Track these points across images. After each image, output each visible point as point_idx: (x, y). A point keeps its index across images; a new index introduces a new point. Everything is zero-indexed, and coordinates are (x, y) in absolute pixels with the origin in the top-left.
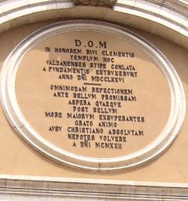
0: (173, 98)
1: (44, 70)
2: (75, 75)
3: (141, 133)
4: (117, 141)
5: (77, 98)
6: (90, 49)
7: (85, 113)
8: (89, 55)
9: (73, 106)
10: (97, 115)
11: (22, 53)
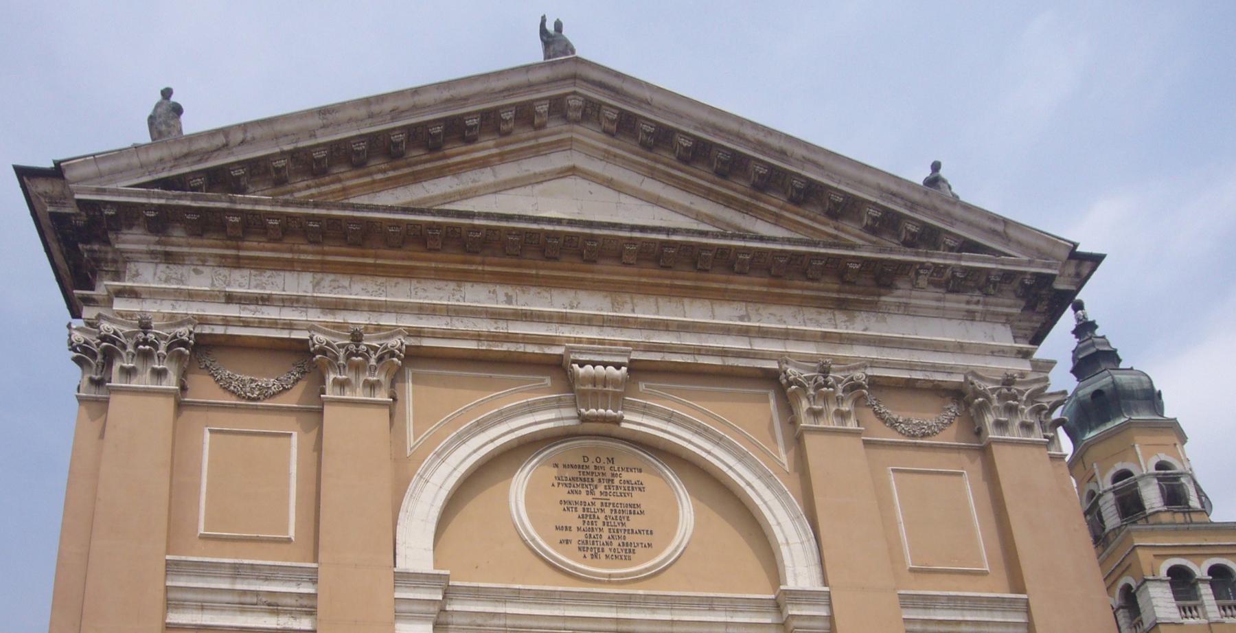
0: (681, 512)
1: (553, 485)
2: (584, 491)
3: (650, 545)
4: (627, 553)
5: (586, 513)
6: (598, 465)
7: (594, 527)
8: (597, 471)
9: (582, 520)
10: (606, 528)
11: (531, 470)
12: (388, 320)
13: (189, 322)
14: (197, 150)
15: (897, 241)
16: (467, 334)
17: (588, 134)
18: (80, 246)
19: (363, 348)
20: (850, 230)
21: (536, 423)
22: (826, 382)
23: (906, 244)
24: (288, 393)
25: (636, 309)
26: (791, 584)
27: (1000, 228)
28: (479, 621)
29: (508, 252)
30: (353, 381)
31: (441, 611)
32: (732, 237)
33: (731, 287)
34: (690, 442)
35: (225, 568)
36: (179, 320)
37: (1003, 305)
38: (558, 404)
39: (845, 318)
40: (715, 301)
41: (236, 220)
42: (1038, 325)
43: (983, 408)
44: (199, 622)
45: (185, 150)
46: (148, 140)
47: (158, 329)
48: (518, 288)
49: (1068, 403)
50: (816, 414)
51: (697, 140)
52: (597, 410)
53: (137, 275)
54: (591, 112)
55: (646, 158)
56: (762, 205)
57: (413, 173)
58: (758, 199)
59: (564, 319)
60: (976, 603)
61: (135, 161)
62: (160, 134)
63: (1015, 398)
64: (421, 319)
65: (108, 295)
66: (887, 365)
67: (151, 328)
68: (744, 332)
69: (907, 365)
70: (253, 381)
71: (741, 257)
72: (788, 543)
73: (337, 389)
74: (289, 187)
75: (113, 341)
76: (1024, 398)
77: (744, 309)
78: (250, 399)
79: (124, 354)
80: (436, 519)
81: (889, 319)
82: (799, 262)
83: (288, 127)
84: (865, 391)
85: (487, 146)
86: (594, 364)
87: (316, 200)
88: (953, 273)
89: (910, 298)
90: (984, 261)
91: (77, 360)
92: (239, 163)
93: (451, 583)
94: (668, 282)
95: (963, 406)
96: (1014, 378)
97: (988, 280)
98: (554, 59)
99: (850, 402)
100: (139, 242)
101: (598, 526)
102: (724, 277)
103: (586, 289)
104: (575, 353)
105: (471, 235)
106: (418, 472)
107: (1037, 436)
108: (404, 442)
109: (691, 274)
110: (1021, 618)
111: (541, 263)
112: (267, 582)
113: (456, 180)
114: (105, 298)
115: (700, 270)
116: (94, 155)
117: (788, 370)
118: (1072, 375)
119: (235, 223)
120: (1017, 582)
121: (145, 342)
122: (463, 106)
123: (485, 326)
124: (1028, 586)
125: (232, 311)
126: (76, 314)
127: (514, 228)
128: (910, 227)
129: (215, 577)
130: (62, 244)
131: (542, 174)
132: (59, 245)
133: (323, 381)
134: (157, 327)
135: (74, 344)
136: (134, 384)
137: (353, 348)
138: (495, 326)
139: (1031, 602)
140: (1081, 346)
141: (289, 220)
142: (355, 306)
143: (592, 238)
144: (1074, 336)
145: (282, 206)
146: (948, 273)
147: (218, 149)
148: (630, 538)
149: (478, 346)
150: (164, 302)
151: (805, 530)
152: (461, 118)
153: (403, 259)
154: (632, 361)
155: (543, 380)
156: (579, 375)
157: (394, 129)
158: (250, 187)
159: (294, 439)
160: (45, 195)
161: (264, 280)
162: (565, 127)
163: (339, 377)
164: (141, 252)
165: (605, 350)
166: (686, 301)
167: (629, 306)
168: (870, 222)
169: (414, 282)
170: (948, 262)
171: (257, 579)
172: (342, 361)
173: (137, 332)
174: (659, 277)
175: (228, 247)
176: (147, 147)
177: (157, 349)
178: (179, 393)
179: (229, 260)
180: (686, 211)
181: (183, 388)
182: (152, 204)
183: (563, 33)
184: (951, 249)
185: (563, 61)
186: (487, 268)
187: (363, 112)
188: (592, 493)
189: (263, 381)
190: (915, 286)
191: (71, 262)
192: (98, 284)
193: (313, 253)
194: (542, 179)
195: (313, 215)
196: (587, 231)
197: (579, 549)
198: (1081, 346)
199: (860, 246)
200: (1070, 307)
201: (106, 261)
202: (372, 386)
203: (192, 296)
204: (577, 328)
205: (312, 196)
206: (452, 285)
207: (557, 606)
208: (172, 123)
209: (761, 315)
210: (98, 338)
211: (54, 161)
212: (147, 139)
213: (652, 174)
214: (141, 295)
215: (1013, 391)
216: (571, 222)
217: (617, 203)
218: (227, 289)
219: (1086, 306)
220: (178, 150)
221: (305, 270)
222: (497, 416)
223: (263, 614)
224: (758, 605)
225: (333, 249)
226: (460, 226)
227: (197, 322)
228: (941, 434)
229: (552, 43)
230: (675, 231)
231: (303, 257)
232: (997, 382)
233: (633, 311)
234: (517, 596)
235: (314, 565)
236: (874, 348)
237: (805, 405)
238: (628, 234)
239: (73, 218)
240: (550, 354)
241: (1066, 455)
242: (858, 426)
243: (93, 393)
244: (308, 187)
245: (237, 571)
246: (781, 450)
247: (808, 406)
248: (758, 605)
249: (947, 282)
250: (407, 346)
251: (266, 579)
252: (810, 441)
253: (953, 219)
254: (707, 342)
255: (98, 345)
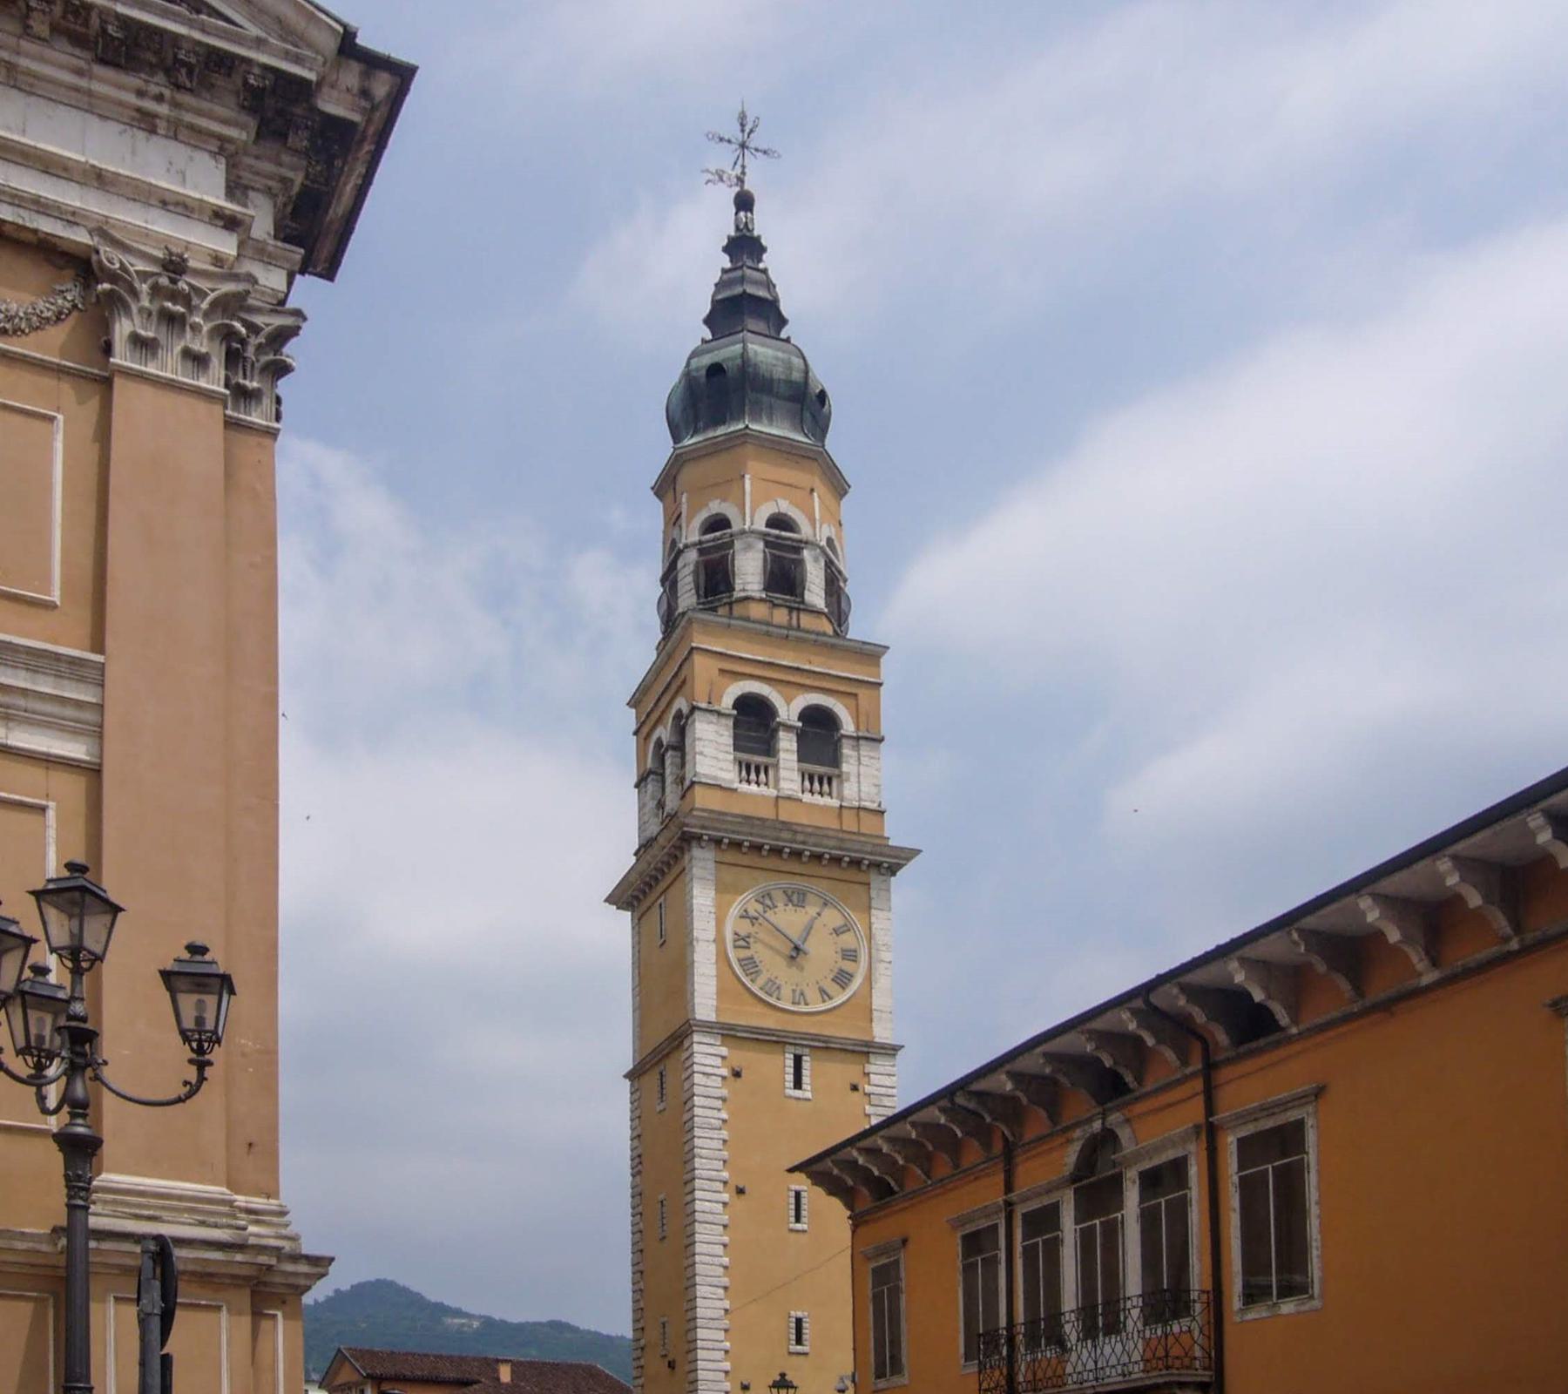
43: (114, 304)
63: (186, 300)
76: (205, 305)
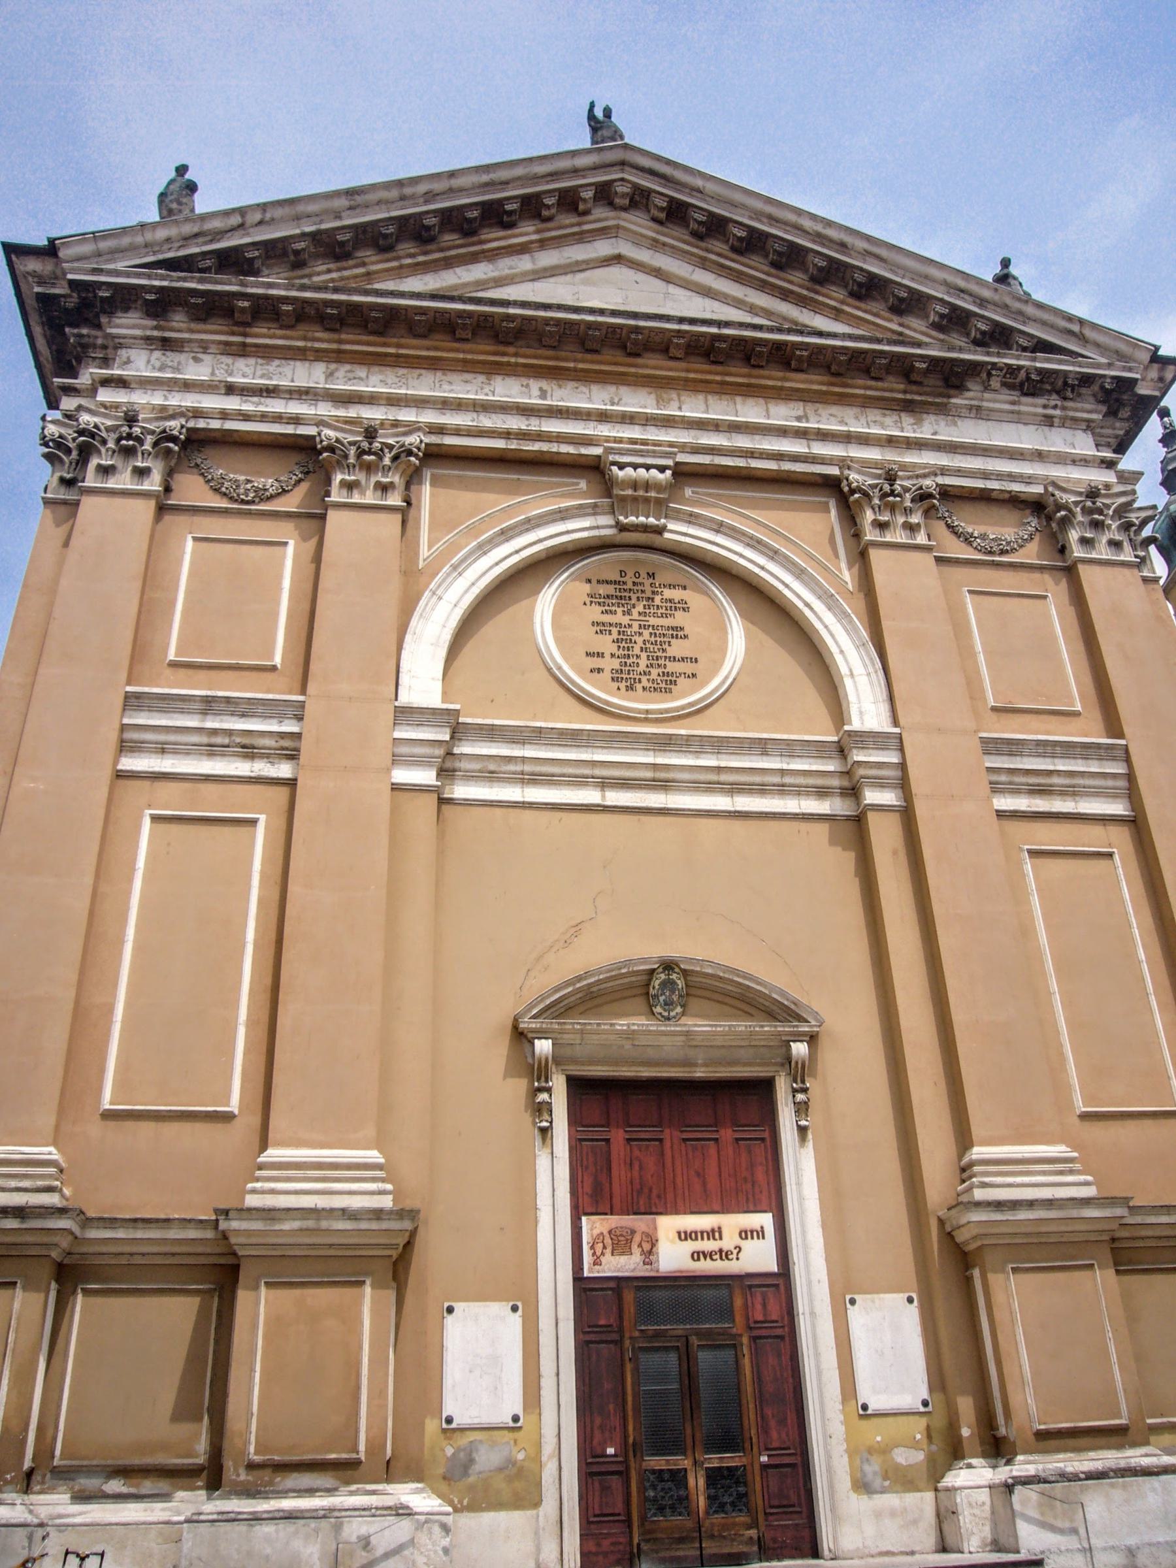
0: (730, 636)
1: (585, 604)
2: (619, 610)
3: (694, 675)
4: (667, 684)
5: (621, 636)
6: (636, 580)
7: (630, 653)
8: (635, 588)
9: (616, 644)
10: (644, 655)
11: (560, 586)
12: (407, 415)
13: (182, 415)
14: (210, 230)
15: (966, 340)
16: (494, 432)
17: (636, 222)
18: (67, 330)
19: (376, 445)
20: (916, 327)
21: (568, 532)
22: (892, 491)
23: (977, 343)
24: (288, 495)
25: (684, 407)
26: (856, 724)
27: (1076, 328)
28: (492, 767)
29: (544, 343)
30: (363, 482)
31: (448, 754)
32: (789, 331)
33: (788, 384)
34: (741, 556)
35: (195, 701)
36: (171, 412)
37: (1083, 411)
38: (595, 510)
39: (912, 421)
40: (769, 400)
41: (246, 304)
42: (1121, 433)
43: (1066, 522)
44: (157, 769)
45: (196, 229)
46: (158, 219)
47: (147, 423)
48: (555, 382)
49: (1159, 518)
50: (882, 526)
51: (751, 230)
52: (637, 518)
53: (128, 361)
54: (639, 199)
55: (697, 247)
56: (821, 298)
57: (445, 259)
58: (817, 292)
59: (603, 417)
60: (1068, 750)
61: (139, 239)
62: (171, 212)
63: (1101, 512)
64: (444, 414)
65: (92, 384)
66: (959, 472)
67: (137, 421)
68: (802, 434)
69: (980, 473)
70: (248, 481)
71: (798, 353)
72: (852, 675)
73: (344, 492)
74: (307, 271)
75: (93, 435)
76: (1111, 512)
77: (802, 409)
78: (243, 502)
79: (103, 450)
80: (448, 643)
81: (959, 423)
82: (861, 360)
83: (312, 208)
84: (935, 501)
85: (527, 231)
86: (635, 466)
87: (336, 284)
88: (1027, 374)
89: (982, 400)
90: (1060, 362)
91: (48, 456)
92: (253, 244)
93: (461, 720)
94: (718, 378)
95: (1044, 520)
96: (1099, 490)
97: (1065, 384)
98: (602, 145)
99: (919, 513)
100: (133, 327)
101: (634, 653)
102: (780, 374)
103: (629, 385)
104: (615, 453)
105: (505, 324)
106: (431, 586)
107: (1127, 555)
108: (417, 554)
109: (745, 370)
110: (1119, 768)
111: (580, 356)
112: (243, 719)
113: (491, 266)
114: (89, 387)
115: (754, 366)
116: (93, 233)
117: (851, 477)
118: (1162, 489)
119: (245, 307)
120: (1113, 726)
121: (129, 436)
122: (503, 190)
123: (515, 423)
124: (1126, 730)
125: (233, 403)
126: (53, 404)
127: (552, 318)
128: (979, 325)
129: (182, 712)
130: (46, 328)
131: (584, 262)
132: (43, 329)
133: (328, 481)
134: (146, 420)
135: (47, 439)
136: (111, 484)
137: (365, 445)
138: (527, 423)
139: (1131, 750)
140: (1170, 455)
141: (305, 305)
142: (371, 400)
143: (637, 330)
144: (1161, 445)
145: (298, 290)
146: (1023, 374)
147: (233, 229)
148: (672, 667)
149: (507, 444)
150: (155, 392)
151: (871, 660)
152: (501, 202)
153: (428, 349)
154: (677, 464)
155: (578, 484)
156: (617, 478)
157: (427, 212)
158: (264, 269)
159: (290, 549)
160: (34, 274)
161: (271, 369)
162: (612, 214)
163: (347, 477)
164: (135, 338)
165: (648, 451)
166: (739, 399)
167: (676, 404)
168: (937, 319)
169: (439, 374)
170: (1022, 363)
171: (232, 715)
172: (352, 460)
173: (121, 426)
174: (710, 373)
175: (233, 334)
176: (154, 226)
177: (142, 445)
178: (162, 494)
179: (234, 348)
180: (738, 303)
181: (168, 489)
182: (154, 287)
183: (613, 119)
184: (1024, 349)
185: (611, 148)
186: (521, 360)
187: (394, 193)
188: (629, 613)
189: (259, 482)
190: (987, 388)
191: (54, 347)
192: (82, 372)
193: (328, 341)
194: (584, 267)
195: (332, 300)
196: (632, 322)
197: (613, 679)
198: (1170, 455)
199: (927, 344)
200: (1155, 415)
201: (94, 346)
202: (384, 488)
203: (187, 386)
204: (618, 426)
205: (333, 280)
206: (481, 378)
207: (585, 749)
208: (184, 200)
209: (820, 416)
210: (75, 432)
211: (49, 239)
212: (153, 216)
213: (703, 264)
214: (130, 384)
215: (1098, 504)
216: (614, 313)
217: (665, 294)
218: (229, 379)
219: (1172, 413)
220: (188, 229)
221: (317, 360)
222: (524, 523)
223: (236, 758)
224: (818, 749)
225: (351, 337)
226: (492, 315)
227: (191, 414)
228: (1021, 551)
229: (601, 128)
230: (727, 324)
231: (317, 345)
232: (1080, 494)
233: (680, 409)
234: (538, 736)
235: (301, 698)
236: (944, 454)
237: (869, 516)
238: (676, 327)
239: (63, 299)
240: (587, 455)
241: (1160, 578)
242: (929, 540)
243: (63, 494)
244: (329, 271)
245: (209, 705)
246: (844, 565)
247: (873, 517)
248: (818, 749)
249: (1022, 384)
250: (427, 444)
251: (243, 715)
252: (876, 557)
253: (1027, 319)
254: (761, 444)
255: (74, 440)
